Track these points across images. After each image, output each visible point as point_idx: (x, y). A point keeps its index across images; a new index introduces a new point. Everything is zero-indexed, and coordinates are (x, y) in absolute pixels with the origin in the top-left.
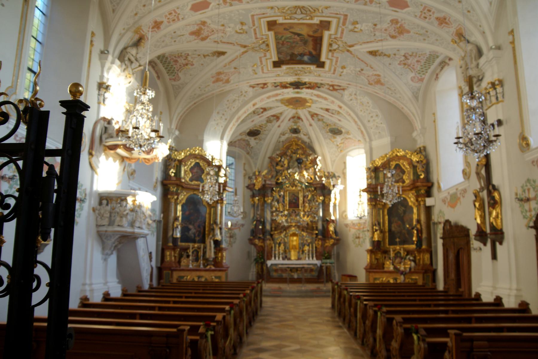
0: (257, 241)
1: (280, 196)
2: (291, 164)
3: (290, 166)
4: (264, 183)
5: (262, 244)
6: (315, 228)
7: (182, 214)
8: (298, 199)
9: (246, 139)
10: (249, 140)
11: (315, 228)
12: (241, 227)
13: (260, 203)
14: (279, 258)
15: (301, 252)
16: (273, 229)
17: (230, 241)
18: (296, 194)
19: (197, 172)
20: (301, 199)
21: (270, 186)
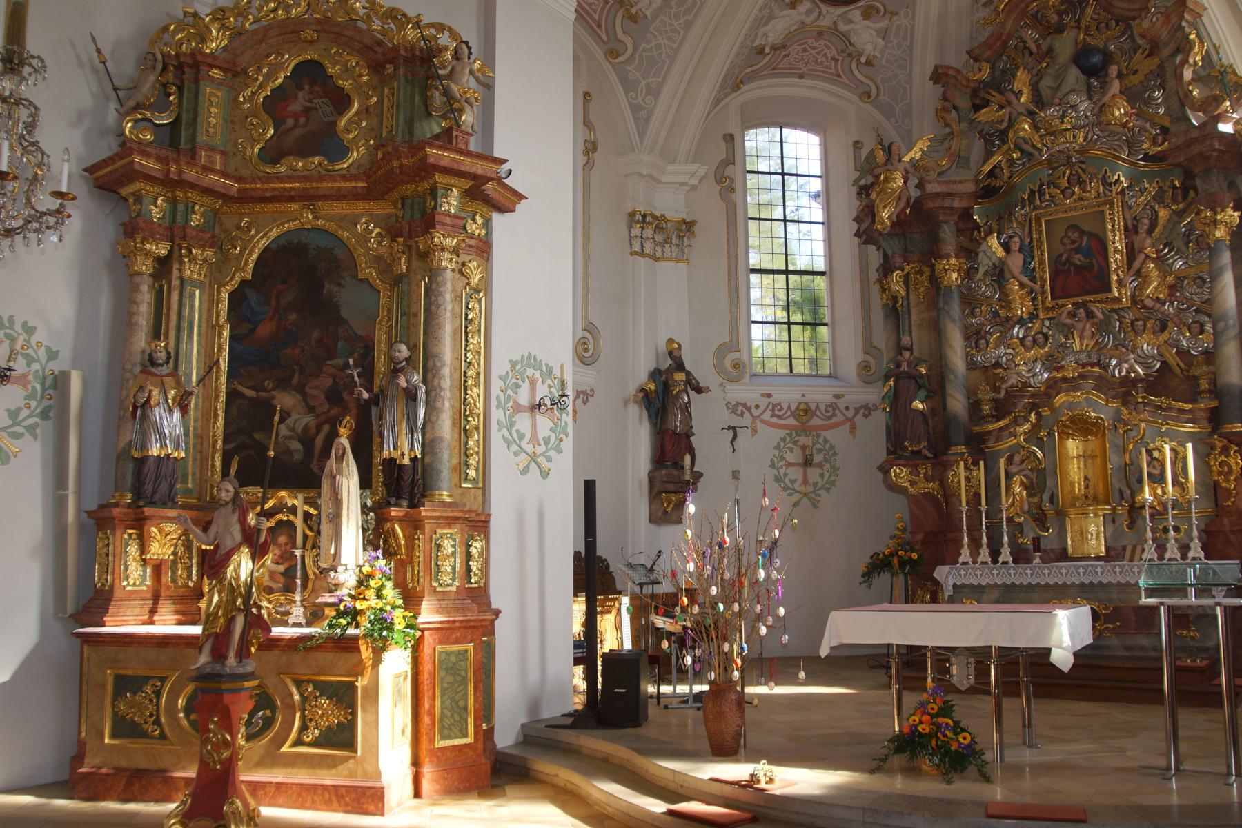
0: (900, 474)
1: (1006, 247)
2: (1046, 82)
3: (1045, 92)
4: (914, 193)
5: (932, 486)
6: (1204, 384)
7: (232, 337)
8: (1102, 246)
9: (825, 22)
10: (843, 28)
11: (1204, 384)
12: (859, 419)
13: (912, 297)
14: (995, 554)
15: (1123, 521)
16: (986, 409)
17: (805, 482)
18: (1087, 227)
19: (307, 111)
20: (1117, 242)
21: (947, 203)
